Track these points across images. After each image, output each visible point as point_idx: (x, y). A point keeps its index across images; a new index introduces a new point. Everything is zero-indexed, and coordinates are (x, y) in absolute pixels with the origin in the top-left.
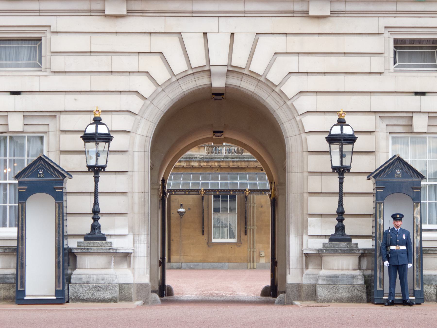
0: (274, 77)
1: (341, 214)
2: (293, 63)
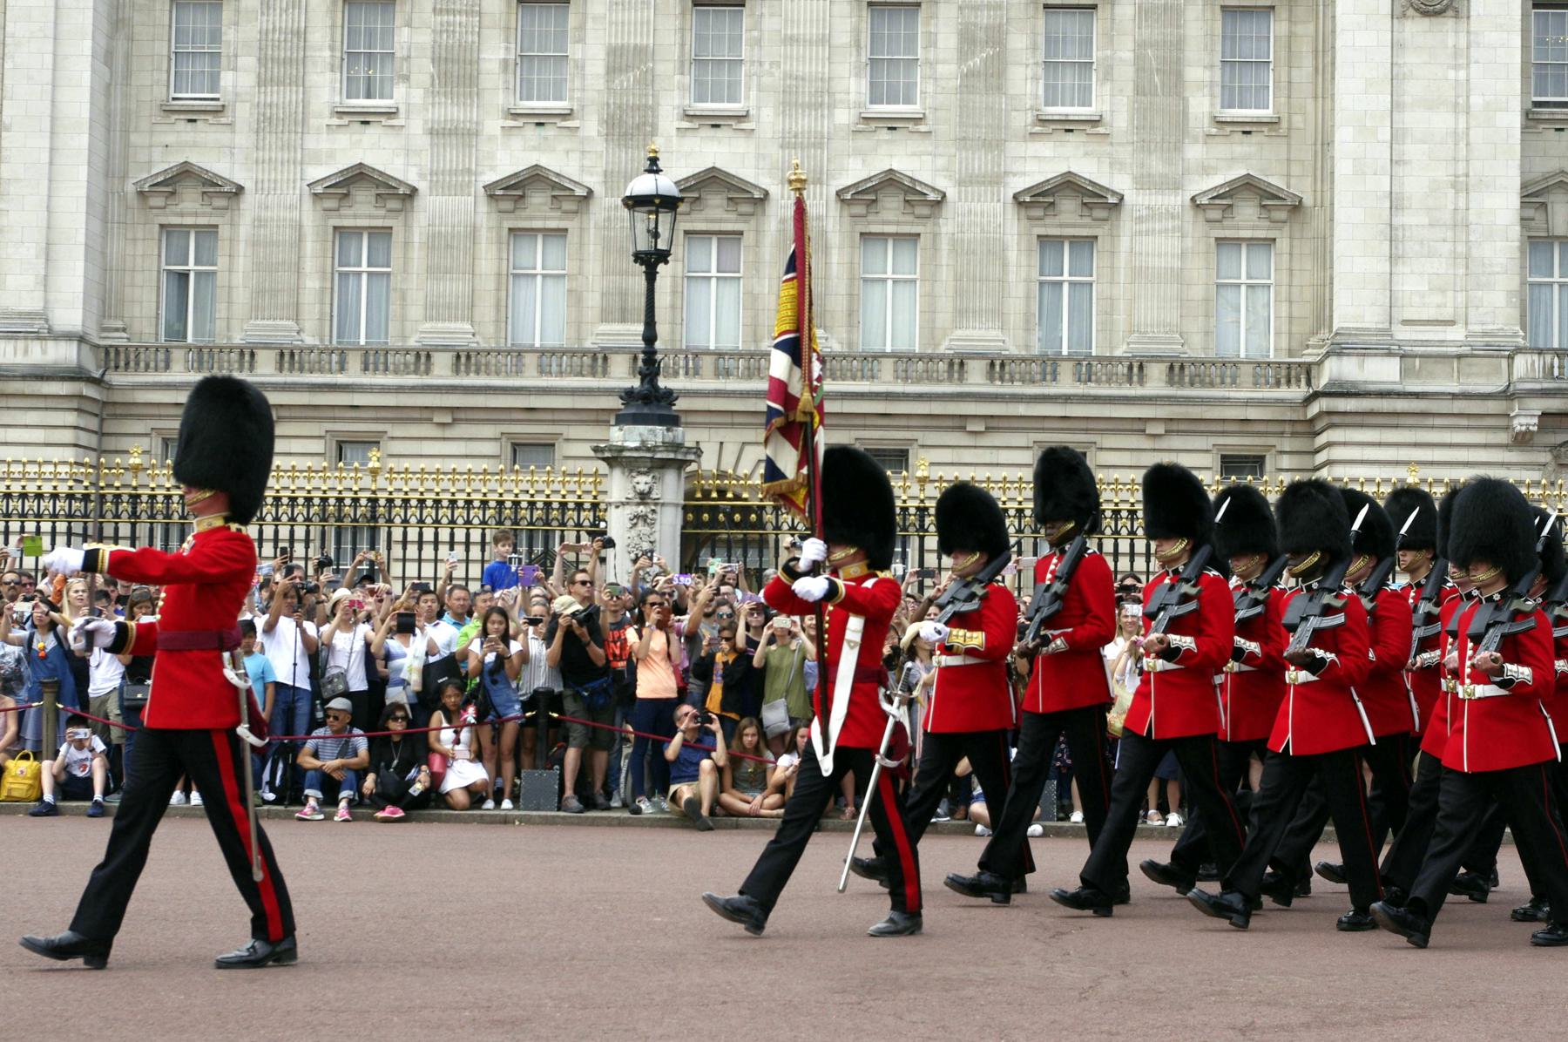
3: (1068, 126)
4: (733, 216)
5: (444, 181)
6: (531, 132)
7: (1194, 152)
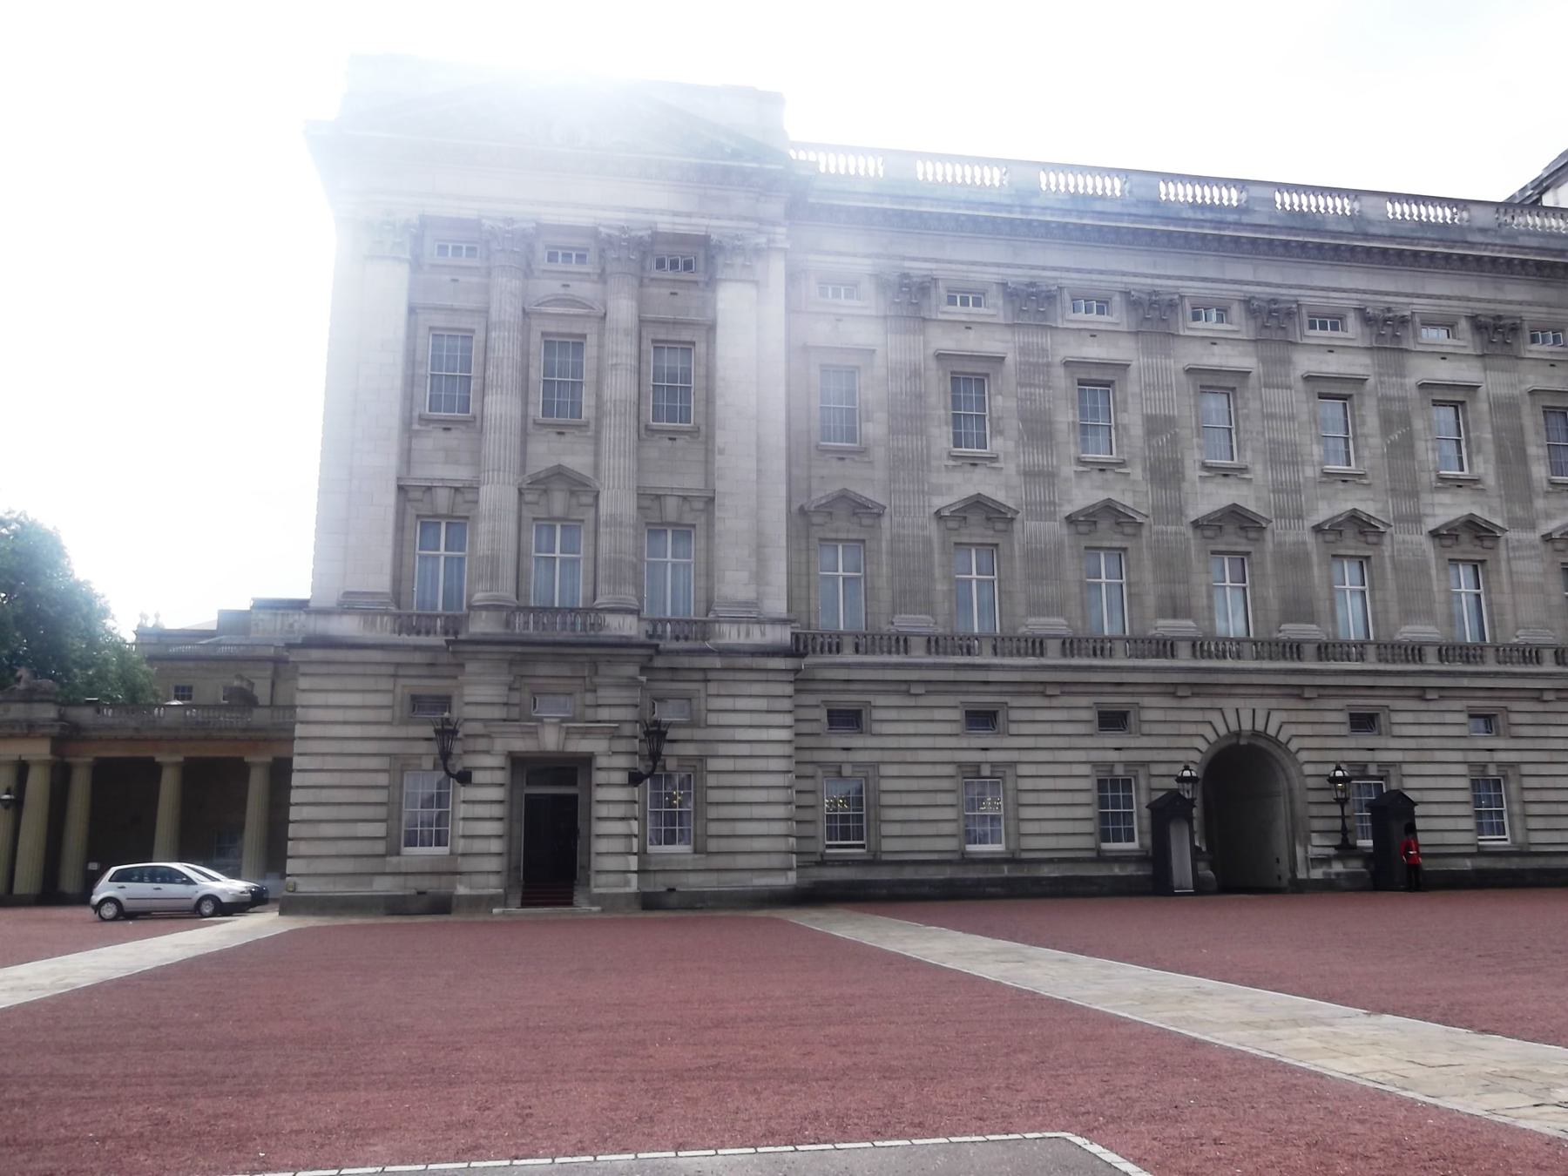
0: (1282, 738)
1: (1344, 831)
2: (1293, 730)
3: (1459, 483)
4: (1244, 541)
5: (1044, 511)
6: (1096, 476)
7: (1540, 504)
